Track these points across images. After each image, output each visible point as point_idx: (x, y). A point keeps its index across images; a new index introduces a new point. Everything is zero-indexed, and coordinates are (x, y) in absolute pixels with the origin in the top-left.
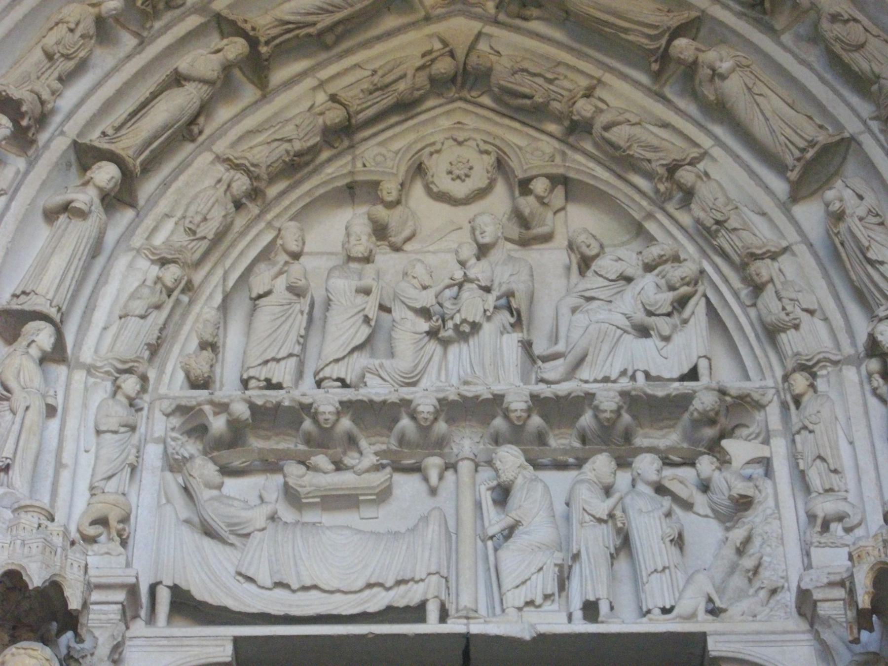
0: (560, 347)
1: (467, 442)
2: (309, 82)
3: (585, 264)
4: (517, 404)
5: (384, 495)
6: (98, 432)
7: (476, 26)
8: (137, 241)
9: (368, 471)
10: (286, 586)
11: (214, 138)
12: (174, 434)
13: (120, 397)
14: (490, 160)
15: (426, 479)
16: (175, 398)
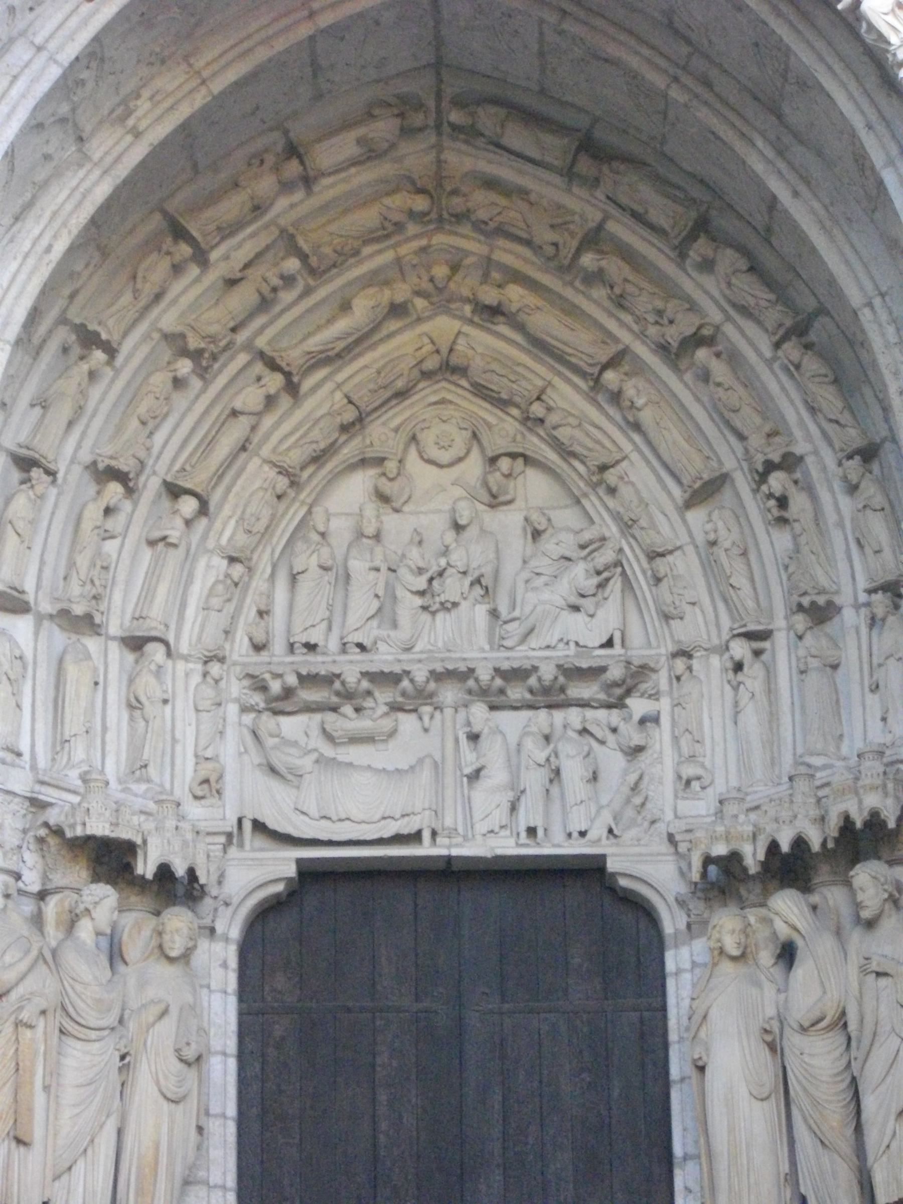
0: (517, 613)
1: (449, 694)
2: (329, 386)
3: (536, 534)
4: (484, 674)
5: (392, 733)
6: (197, 710)
7: (456, 325)
8: (211, 544)
9: (381, 717)
10: (330, 819)
11: (260, 445)
12: (245, 691)
13: (209, 679)
14: (467, 434)
15: (421, 718)
16: (244, 665)
